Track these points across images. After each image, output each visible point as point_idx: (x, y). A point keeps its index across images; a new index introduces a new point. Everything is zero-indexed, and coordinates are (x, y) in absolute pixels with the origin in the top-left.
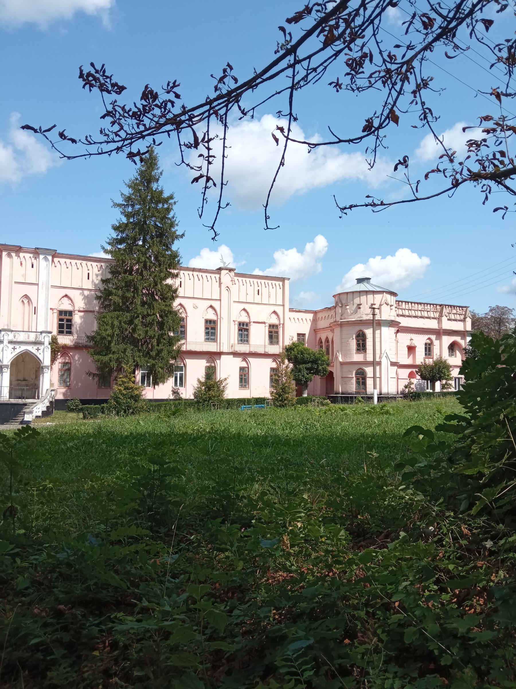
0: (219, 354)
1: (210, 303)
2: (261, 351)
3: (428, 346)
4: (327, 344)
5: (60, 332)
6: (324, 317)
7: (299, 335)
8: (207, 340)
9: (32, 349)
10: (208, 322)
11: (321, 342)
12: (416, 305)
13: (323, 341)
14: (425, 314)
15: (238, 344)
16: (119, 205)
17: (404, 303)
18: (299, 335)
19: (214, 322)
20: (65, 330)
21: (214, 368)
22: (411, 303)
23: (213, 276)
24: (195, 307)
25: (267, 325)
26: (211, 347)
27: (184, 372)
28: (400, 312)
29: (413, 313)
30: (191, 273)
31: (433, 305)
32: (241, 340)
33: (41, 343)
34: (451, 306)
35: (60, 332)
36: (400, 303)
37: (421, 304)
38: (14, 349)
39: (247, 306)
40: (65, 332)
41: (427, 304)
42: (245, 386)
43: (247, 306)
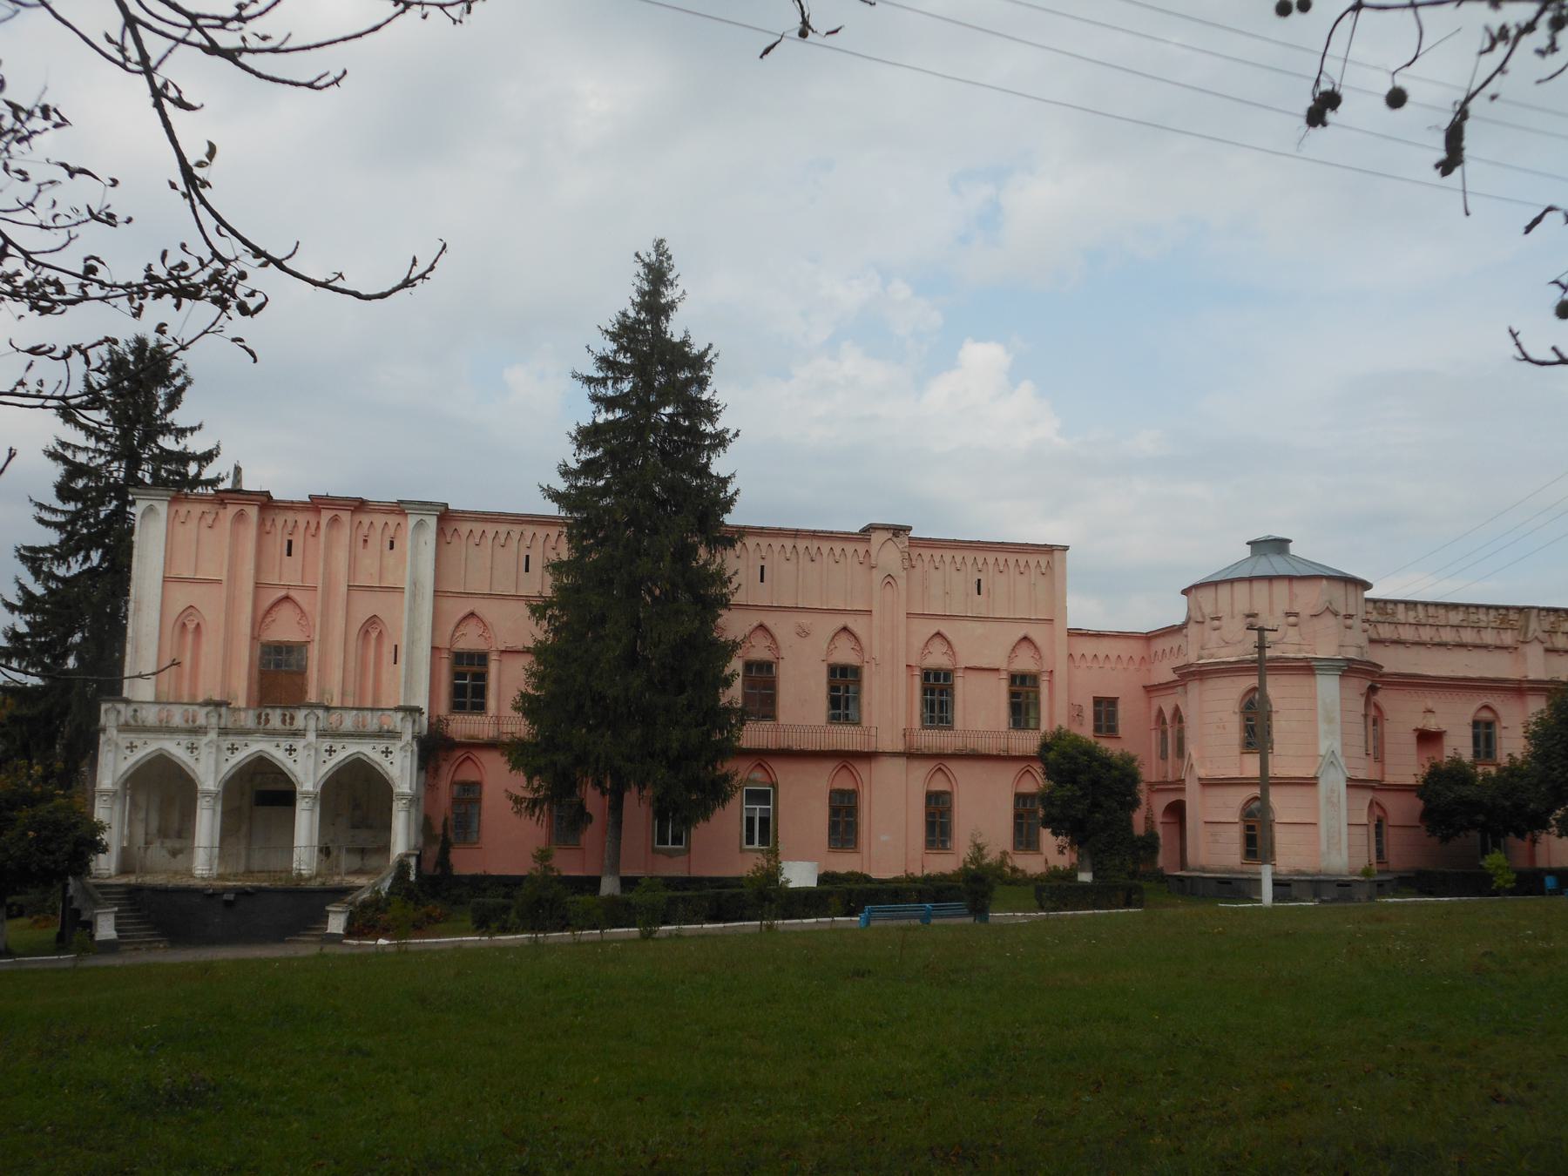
0: (869, 756)
1: (840, 621)
2: (986, 745)
3: (1482, 731)
4: (1177, 726)
5: (458, 706)
6: (1168, 651)
7: (1098, 701)
8: (834, 719)
9: (370, 751)
11: (1164, 722)
12: (1442, 611)
13: (1168, 716)
14: (1468, 636)
15: (924, 727)
16: (589, 380)
17: (1401, 607)
18: (1098, 701)
20: (468, 700)
21: (852, 795)
22: (1426, 604)
23: (850, 547)
24: (803, 633)
25: (1004, 675)
26: (845, 739)
27: (771, 807)
28: (1385, 632)
29: (1426, 634)
30: (789, 543)
31: (1497, 608)
33: (393, 735)
34: (1556, 610)
35: (458, 706)
36: (1390, 606)
37: (1455, 607)
38: (331, 751)
39: (943, 627)
40: (468, 705)
41: (1477, 607)
42: (944, 843)
43: (943, 627)
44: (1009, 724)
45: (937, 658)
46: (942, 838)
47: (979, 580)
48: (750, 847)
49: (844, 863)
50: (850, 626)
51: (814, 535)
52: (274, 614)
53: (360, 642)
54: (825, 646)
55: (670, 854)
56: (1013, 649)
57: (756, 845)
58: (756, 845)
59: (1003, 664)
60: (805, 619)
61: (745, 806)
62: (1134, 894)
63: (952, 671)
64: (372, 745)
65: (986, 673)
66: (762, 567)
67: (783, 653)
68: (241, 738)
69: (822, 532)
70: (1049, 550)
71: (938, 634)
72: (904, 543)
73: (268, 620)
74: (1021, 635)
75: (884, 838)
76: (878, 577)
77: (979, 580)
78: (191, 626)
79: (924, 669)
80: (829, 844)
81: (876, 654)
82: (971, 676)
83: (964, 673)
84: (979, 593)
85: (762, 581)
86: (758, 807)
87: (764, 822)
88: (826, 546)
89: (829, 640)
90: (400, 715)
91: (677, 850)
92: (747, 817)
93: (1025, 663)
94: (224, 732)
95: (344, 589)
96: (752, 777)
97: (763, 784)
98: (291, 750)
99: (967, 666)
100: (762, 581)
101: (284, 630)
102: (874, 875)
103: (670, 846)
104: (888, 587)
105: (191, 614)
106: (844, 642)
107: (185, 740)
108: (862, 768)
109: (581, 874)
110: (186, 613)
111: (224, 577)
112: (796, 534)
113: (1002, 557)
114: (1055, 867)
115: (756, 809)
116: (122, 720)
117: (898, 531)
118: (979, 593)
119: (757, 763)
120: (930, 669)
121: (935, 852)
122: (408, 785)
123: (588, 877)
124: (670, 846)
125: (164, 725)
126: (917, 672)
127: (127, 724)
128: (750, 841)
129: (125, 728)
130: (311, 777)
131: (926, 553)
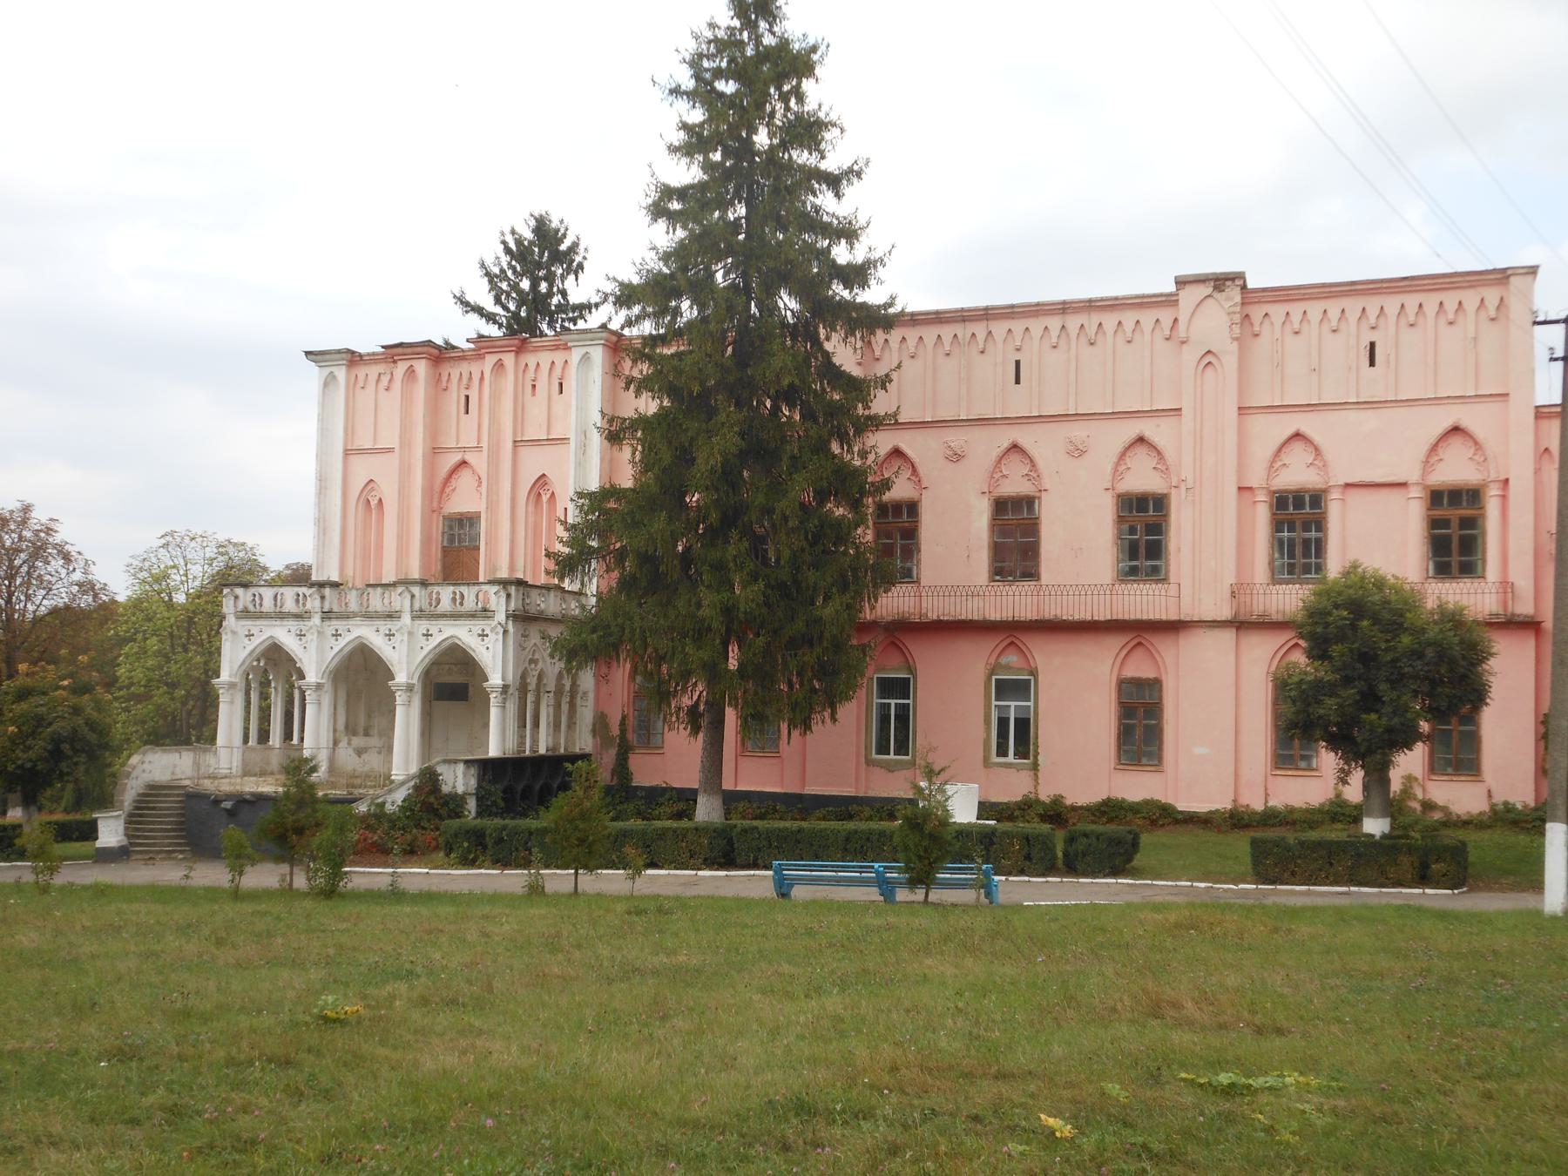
0: (1174, 627)
1: (1131, 429)
10: (1001, 506)
15: (1275, 581)
19: (1159, 503)
21: (1153, 686)
24: (1077, 452)
25: (1415, 492)
26: (1143, 602)
27: (1031, 704)
30: (1054, 323)
32: (1291, 569)
42: (1307, 758)
44: (1427, 570)
45: (1297, 474)
46: (1303, 753)
47: (1372, 345)
48: (1002, 760)
49: (1136, 787)
50: (1148, 434)
51: (1091, 306)
52: (454, 483)
53: (531, 508)
54: (1109, 468)
55: (890, 767)
56: (1434, 448)
57: (1011, 758)
58: (1011, 758)
59: (1410, 472)
60: (1078, 431)
61: (994, 703)
62: (1437, 861)
63: (1325, 491)
64: (467, 628)
65: (1384, 492)
66: (1018, 363)
67: (1046, 484)
68: (344, 623)
69: (1102, 300)
70: (1502, 276)
71: (1297, 436)
72: (1232, 299)
73: (447, 490)
74: (1447, 424)
75: (1200, 751)
76: (1191, 355)
77: (1372, 345)
78: (374, 503)
79: (1275, 492)
80: (1119, 758)
81: (1187, 473)
82: (1355, 497)
83: (1343, 493)
84: (1372, 363)
85: (1018, 381)
86: (1013, 704)
87: (1023, 725)
88: (1110, 320)
89: (1115, 459)
90: (495, 588)
91: (897, 762)
92: (1015, 719)
93: (1455, 469)
94: (327, 615)
95: (510, 445)
96: (1004, 660)
97: (1019, 670)
98: (390, 635)
99: (1350, 481)
100: (1018, 381)
101: (463, 500)
102: (1182, 806)
103: (892, 756)
104: (1210, 370)
105: (373, 489)
106: (1141, 462)
107: (293, 624)
108: (1165, 647)
109: (778, 790)
110: (369, 488)
111: (395, 443)
112: (1064, 308)
113: (1412, 301)
114: (1506, 803)
115: (889, 704)
116: (240, 607)
117: (1220, 282)
118: (1372, 363)
119: (1008, 641)
120: (1286, 491)
121: (1290, 773)
122: (500, 675)
123: (785, 794)
124: (892, 756)
125: (278, 609)
126: (1262, 497)
127: (246, 610)
128: (1002, 751)
129: (245, 614)
130: (405, 666)
131: (1277, 312)
